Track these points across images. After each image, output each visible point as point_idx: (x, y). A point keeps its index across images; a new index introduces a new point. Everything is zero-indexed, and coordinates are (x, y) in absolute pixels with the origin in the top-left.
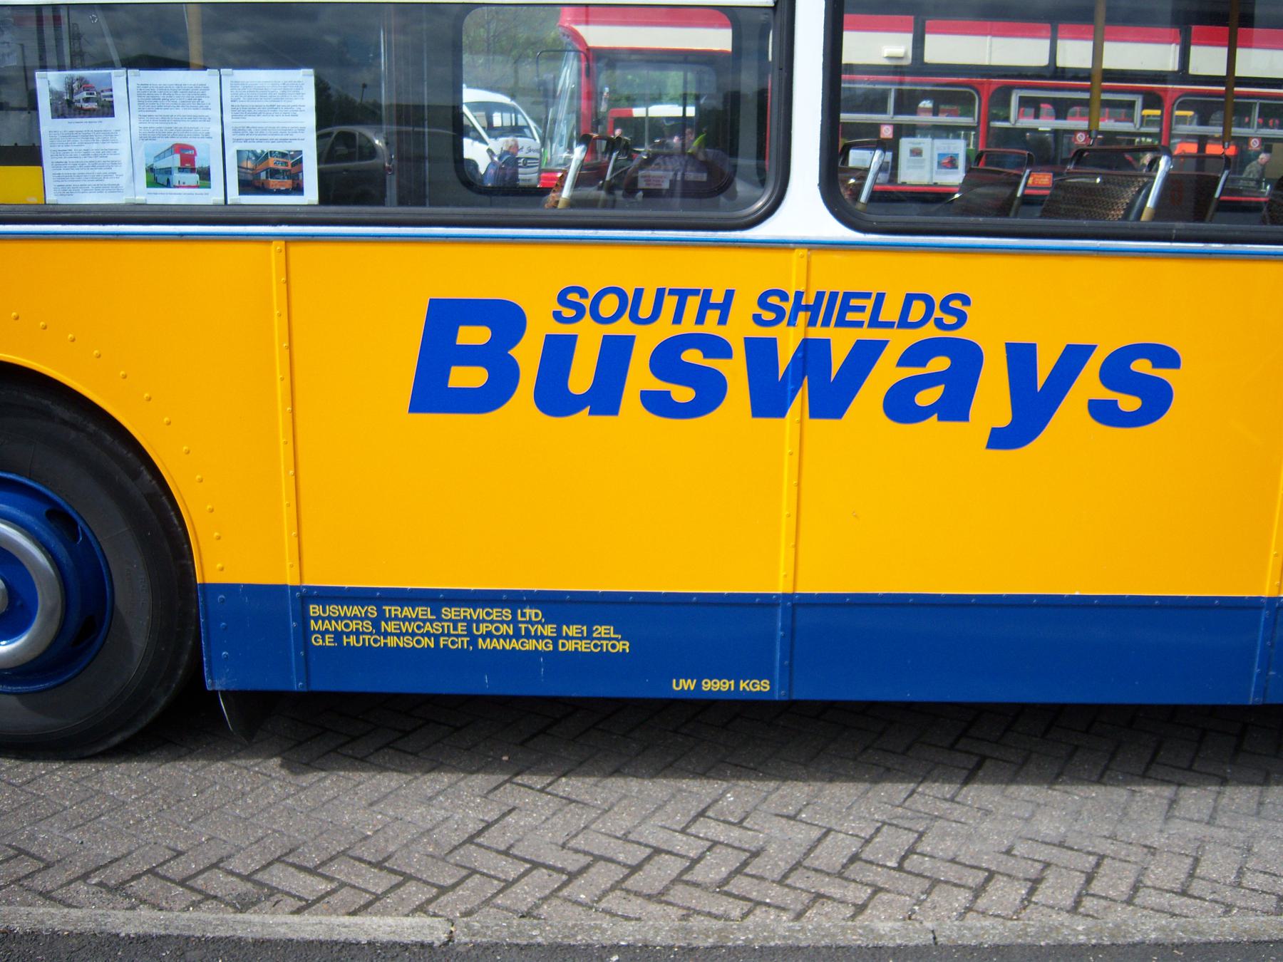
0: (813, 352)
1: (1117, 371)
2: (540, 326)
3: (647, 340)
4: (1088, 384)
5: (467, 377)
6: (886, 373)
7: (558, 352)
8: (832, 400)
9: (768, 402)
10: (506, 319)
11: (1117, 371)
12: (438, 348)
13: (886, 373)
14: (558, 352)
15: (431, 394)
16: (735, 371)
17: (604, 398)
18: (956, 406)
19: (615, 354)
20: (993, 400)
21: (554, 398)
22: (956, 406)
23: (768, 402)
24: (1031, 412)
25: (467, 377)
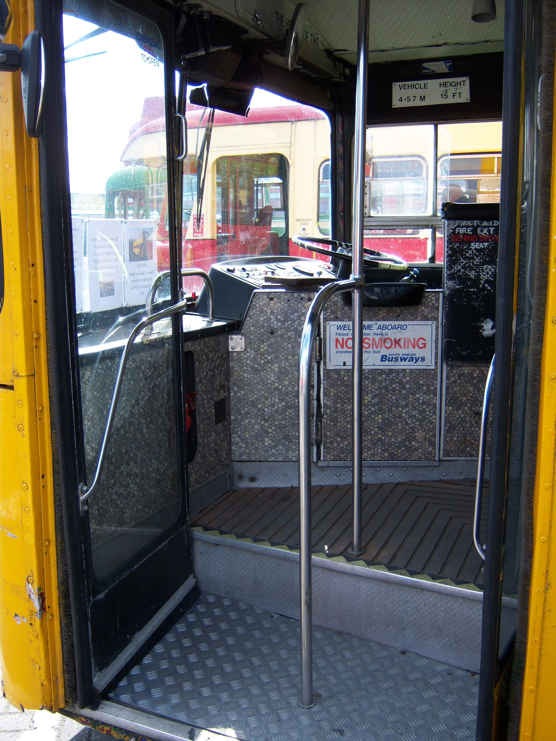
0: (404, 358)
1: (422, 358)
2: (388, 356)
3: (394, 357)
4: (420, 359)
5: (384, 359)
6: (408, 359)
7: (389, 358)
8: (405, 361)
9: (401, 360)
10: (386, 356)
11: (422, 358)
12: (382, 358)
13: (408, 359)
14: (389, 358)
15: (382, 361)
16: (399, 359)
17: (392, 361)
18: (412, 361)
19: (392, 358)
20: (414, 360)
21: (389, 361)
22: (412, 361)
23: (401, 360)
24: (417, 361)
25: (384, 359)
